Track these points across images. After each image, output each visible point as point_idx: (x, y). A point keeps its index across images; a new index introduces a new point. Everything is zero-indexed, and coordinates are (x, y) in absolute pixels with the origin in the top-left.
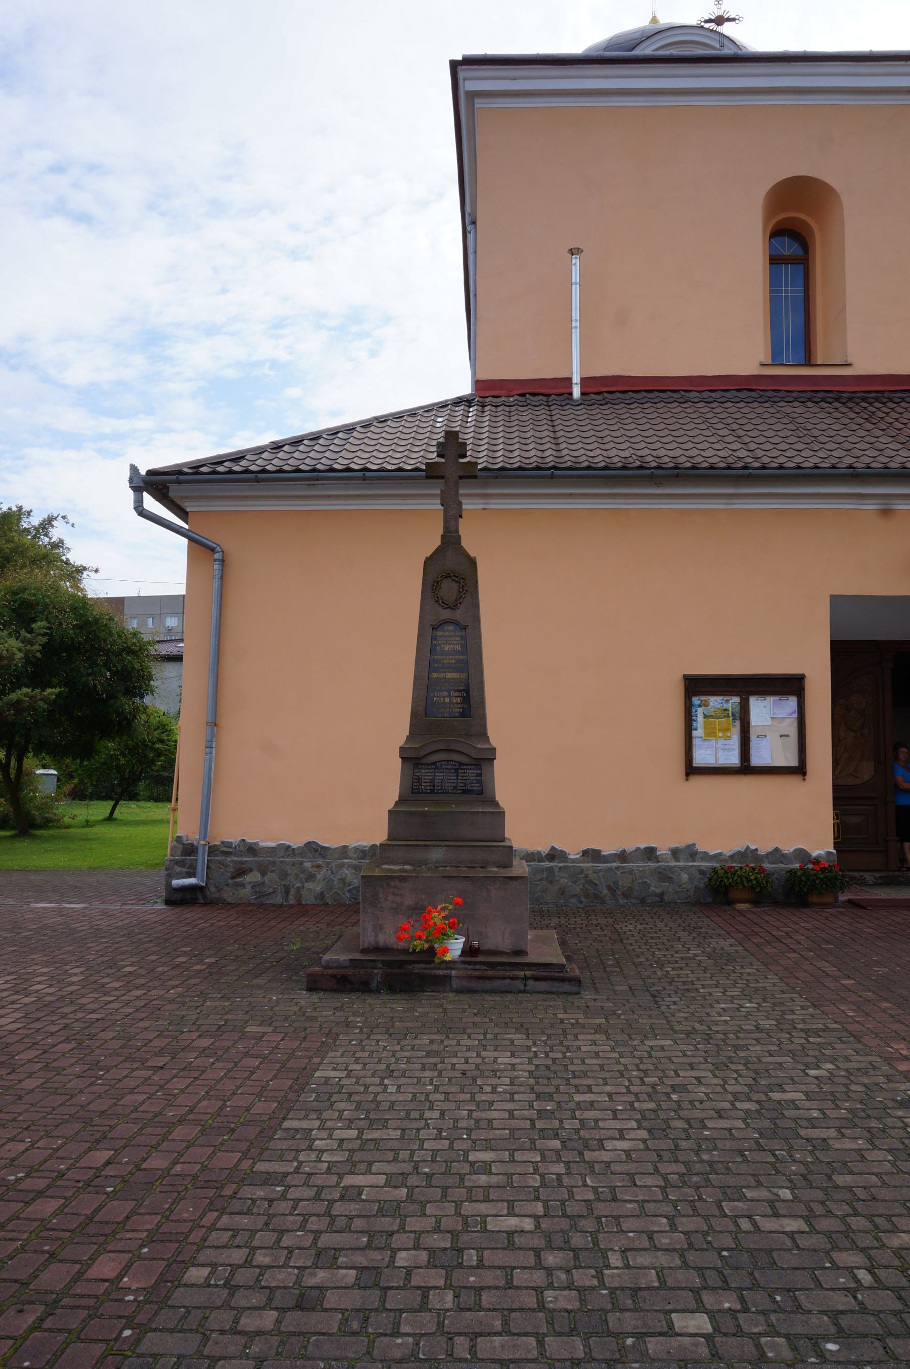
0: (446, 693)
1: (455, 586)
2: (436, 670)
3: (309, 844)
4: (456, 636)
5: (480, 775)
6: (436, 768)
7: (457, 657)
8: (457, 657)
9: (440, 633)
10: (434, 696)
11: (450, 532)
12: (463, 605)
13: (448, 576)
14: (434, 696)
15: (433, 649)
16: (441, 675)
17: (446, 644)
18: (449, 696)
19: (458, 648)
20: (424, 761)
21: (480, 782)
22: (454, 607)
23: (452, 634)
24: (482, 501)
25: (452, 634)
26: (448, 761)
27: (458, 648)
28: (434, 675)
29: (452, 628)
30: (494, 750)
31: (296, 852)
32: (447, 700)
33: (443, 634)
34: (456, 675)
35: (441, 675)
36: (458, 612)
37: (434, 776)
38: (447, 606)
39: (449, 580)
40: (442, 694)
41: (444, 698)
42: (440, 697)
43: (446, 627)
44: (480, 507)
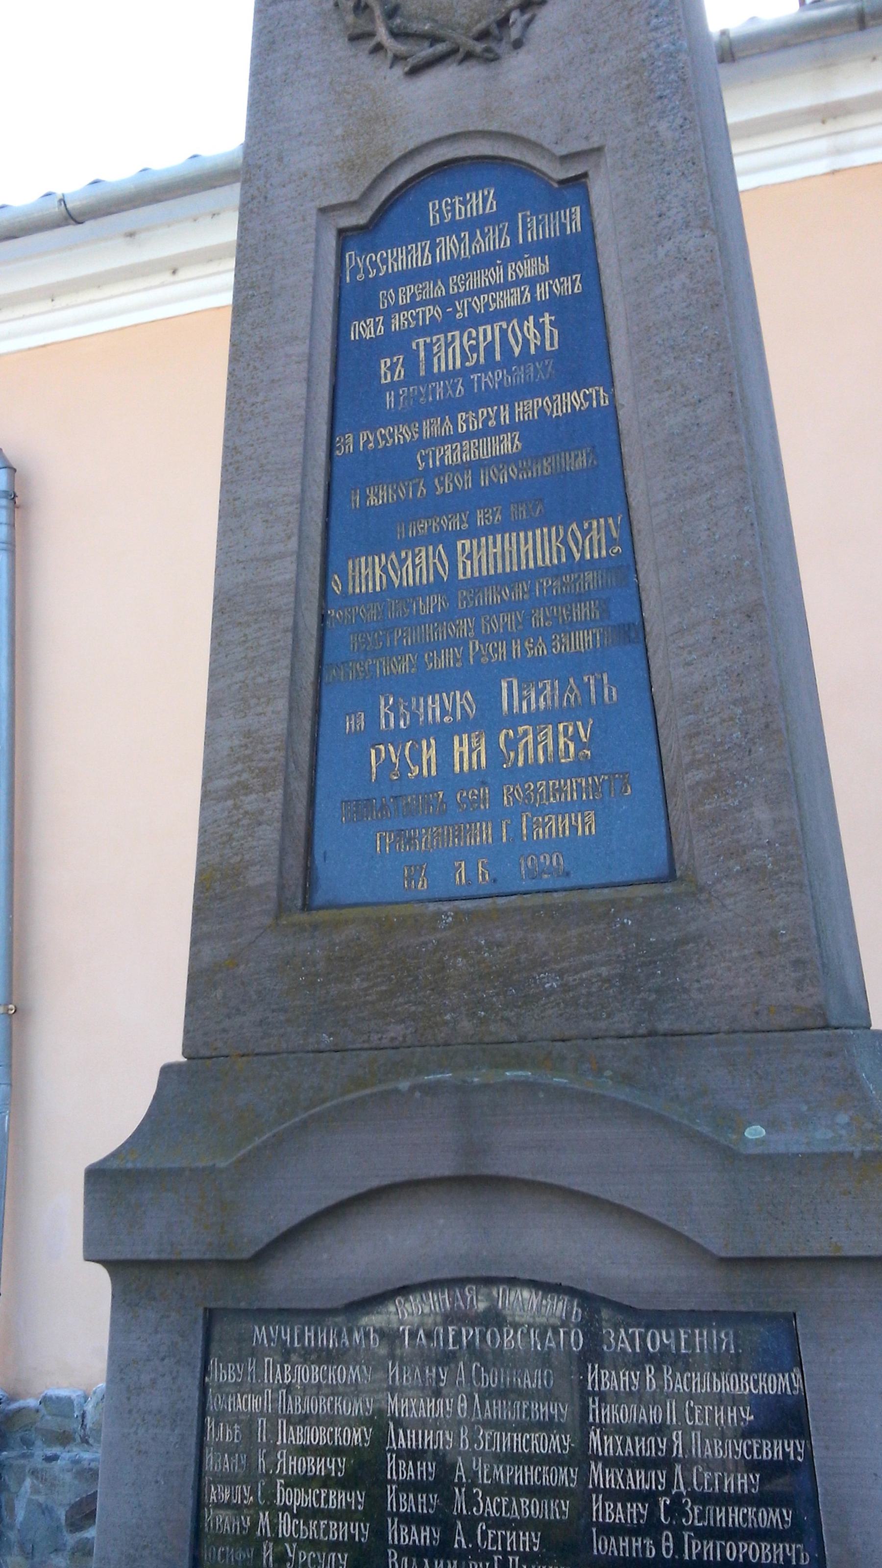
0: (463, 701)
2: (383, 535)
4: (515, 253)
5: (787, 1417)
7: (527, 409)
8: (527, 409)
10: (376, 736)
15: (348, 383)
16: (418, 567)
17: (448, 324)
18: (488, 720)
20: (285, 1281)
23: (493, 240)
24: (822, 145)
25: (493, 240)
27: (539, 334)
28: (368, 573)
32: (468, 753)
33: (418, 256)
34: (535, 548)
35: (418, 567)
36: (519, 68)
40: (432, 708)
41: (444, 735)
42: (417, 732)
44: (821, 167)
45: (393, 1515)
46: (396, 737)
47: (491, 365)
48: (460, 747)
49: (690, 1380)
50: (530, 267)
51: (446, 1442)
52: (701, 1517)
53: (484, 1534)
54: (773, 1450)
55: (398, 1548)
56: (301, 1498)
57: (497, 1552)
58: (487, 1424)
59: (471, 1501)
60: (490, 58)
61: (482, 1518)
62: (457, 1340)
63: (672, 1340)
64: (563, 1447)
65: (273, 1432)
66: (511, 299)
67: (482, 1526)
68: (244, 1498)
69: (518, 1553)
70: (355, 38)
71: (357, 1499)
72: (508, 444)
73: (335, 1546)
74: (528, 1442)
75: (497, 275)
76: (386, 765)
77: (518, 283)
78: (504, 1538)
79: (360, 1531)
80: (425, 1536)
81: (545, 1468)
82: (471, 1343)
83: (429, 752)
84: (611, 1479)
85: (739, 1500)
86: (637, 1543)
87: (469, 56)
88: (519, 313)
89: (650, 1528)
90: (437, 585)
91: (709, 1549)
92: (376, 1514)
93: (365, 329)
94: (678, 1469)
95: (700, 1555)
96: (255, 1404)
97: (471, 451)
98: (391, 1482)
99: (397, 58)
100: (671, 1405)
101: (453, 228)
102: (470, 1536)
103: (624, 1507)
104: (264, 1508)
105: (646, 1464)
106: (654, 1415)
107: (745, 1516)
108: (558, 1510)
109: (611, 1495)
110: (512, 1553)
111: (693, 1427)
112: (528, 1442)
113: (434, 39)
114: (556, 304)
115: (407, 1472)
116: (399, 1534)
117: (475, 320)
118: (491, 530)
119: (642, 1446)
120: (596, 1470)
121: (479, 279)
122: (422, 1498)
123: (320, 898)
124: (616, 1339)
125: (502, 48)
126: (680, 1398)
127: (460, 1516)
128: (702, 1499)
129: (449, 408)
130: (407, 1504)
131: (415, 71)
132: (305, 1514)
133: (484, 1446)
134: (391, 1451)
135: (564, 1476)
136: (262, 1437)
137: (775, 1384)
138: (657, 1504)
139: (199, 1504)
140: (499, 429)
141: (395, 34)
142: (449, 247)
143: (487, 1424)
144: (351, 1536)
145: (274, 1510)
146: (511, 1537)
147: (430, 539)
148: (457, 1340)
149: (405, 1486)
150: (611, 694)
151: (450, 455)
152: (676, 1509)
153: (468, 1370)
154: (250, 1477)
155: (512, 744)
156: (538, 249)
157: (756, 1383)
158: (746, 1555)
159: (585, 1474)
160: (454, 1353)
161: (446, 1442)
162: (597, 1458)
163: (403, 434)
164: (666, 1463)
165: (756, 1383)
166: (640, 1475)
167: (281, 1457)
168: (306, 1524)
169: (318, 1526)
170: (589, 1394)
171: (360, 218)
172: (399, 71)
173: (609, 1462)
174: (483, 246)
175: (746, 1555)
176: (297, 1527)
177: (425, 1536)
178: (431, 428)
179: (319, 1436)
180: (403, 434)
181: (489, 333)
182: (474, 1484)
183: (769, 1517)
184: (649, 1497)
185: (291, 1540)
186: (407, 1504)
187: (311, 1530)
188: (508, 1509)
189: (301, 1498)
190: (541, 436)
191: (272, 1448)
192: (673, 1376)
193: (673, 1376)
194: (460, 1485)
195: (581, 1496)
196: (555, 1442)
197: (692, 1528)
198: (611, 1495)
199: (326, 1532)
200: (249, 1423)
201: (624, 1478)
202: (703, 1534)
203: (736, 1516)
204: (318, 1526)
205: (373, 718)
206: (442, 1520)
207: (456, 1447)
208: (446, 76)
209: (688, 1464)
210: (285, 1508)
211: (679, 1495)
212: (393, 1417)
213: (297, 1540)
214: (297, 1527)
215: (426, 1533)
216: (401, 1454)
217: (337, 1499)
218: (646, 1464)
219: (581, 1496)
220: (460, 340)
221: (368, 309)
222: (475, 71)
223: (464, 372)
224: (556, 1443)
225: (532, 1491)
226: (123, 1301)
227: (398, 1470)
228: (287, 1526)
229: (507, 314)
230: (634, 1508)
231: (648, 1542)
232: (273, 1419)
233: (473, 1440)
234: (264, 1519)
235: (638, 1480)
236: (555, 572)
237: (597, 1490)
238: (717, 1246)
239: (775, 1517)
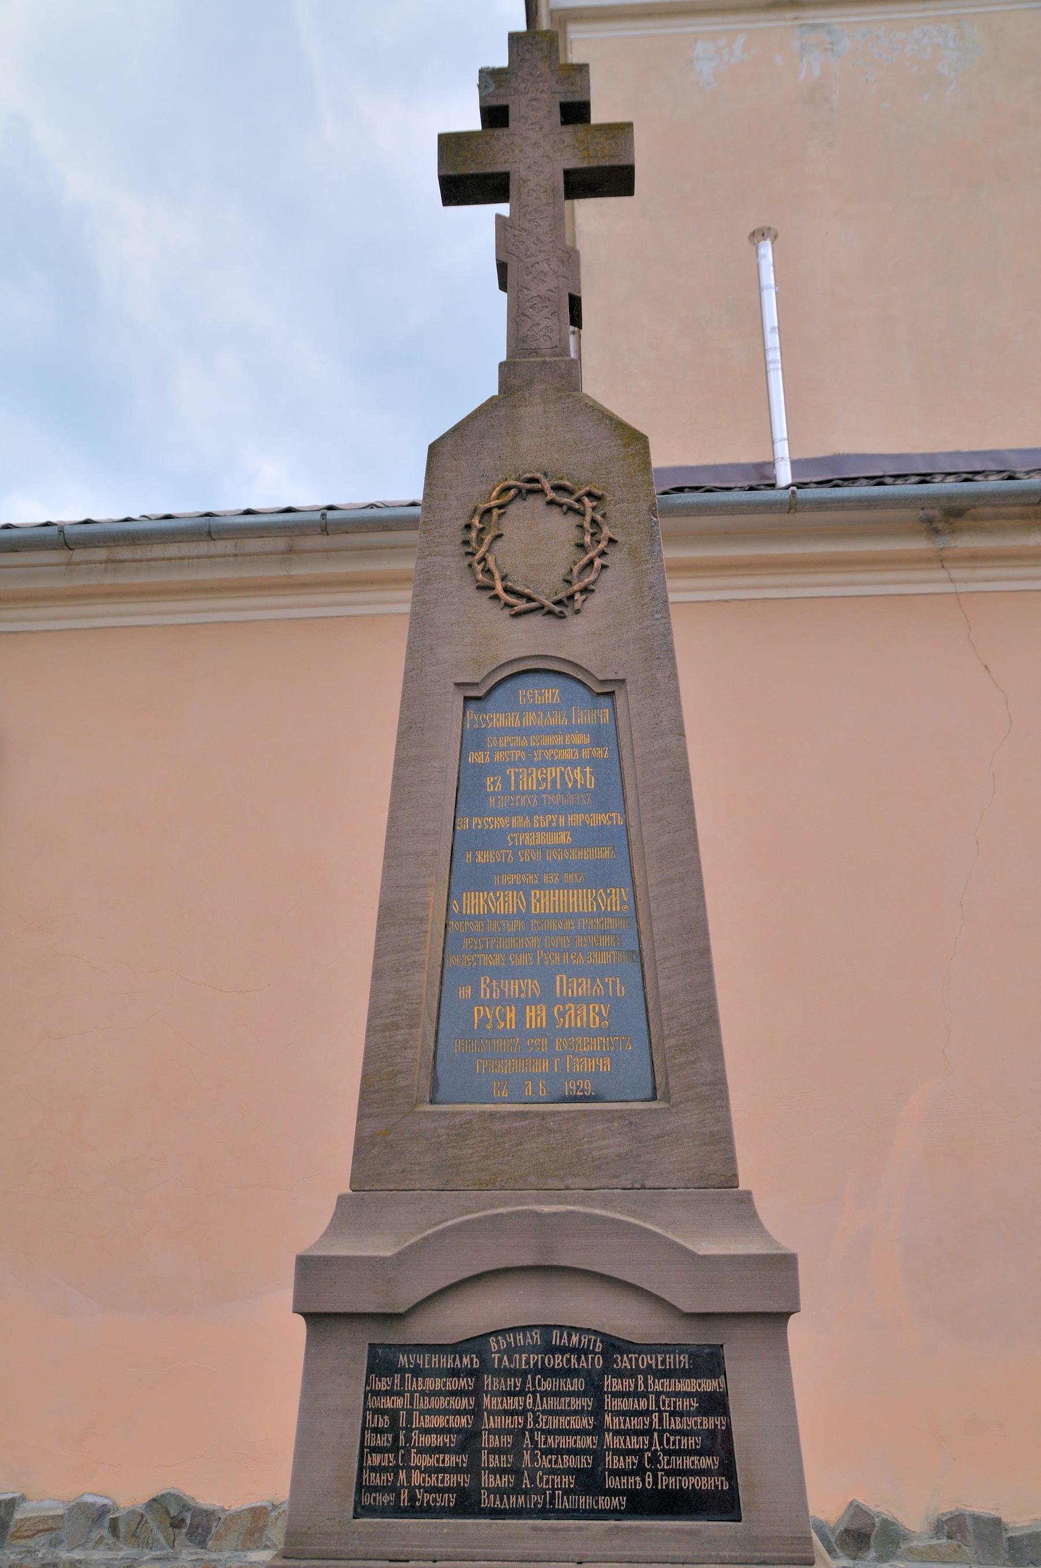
0: (533, 986)
1: (561, 528)
2: (482, 880)
3: (158, 1503)
4: (570, 729)
5: (716, 1404)
6: (485, 1367)
7: (576, 819)
8: (576, 819)
9: (498, 719)
10: (476, 999)
11: (535, 352)
12: (595, 601)
13: (530, 488)
14: (476, 999)
15: (467, 791)
16: (506, 903)
17: (529, 763)
18: (548, 997)
19: (583, 778)
21: (720, 1444)
22: (560, 608)
23: (556, 720)
25: (556, 720)
26: (547, 1329)
27: (583, 778)
28: (474, 902)
29: (550, 693)
30: (785, 1264)
31: (122, 1528)
32: (535, 1017)
34: (579, 900)
35: (506, 903)
36: (576, 626)
37: (476, 1412)
38: (522, 604)
39: (536, 503)
40: (513, 987)
41: (521, 1005)
42: (503, 1001)
43: (530, 692)
45: (485, 1469)
46: (490, 1003)
47: (554, 791)
48: (530, 1012)
49: (663, 1384)
50: (579, 739)
51: (519, 1424)
52: (668, 1463)
53: (541, 1478)
54: (709, 1423)
55: (488, 1489)
56: (428, 1461)
57: (548, 1489)
58: (544, 1412)
59: (534, 1458)
60: (561, 616)
61: (540, 1469)
62: (528, 1363)
63: (654, 1361)
64: (589, 1425)
65: (409, 1421)
66: (567, 755)
67: (540, 1473)
68: (389, 1462)
69: (561, 1489)
70: (482, 588)
71: (464, 1460)
72: (564, 838)
73: (449, 1490)
74: (569, 1422)
75: (560, 741)
76: (484, 1020)
77: (572, 746)
78: (553, 1480)
79: (464, 1480)
80: (505, 1481)
81: (579, 1437)
82: (536, 1364)
83: (511, 1015)
84: (618, 1442)
85: (689, 1453)
86: (631, 1480)
87: (550, 612)
88: (573, 764)
89: (639, 1471)
90: (519, 916)
91: (672, 1482)
92: (474, 1469)
93: (476, 757)
94: (656, 1434)
95: (667, 1486)
96: (399, 1402)
97: (541, 839)
98: (485, 1448)
99: (507, 605)
100: (652, 1397)
101: (534, 708)
102: (532, 1480)
103: (624, 1459)
104: (402, 1468)
105: (637, 1433)
106: (643, 1404)
107: (693, 1462)
108: (584, 1462)
109: (617, 1452)
110: (557, 1489)
111: (665, 1411)
112: (569, 1422)
113: (530, 599)
114: (593, 762)
115: (495, 1442)
116: (489, 1481)
117: (545, 764)
118: (552, 887)
119: (635, 1423)
120: (608, 1437)
121: (549, 740)
122: (503, 1458)
123: (439, 1097)
124: (622, 1361)
125: (567, 612)
126: (658, 1394)
127: (527, 1468)
128: (669, 1453)
129: (528, 812)
130: (494, 1461)
131: (517, 615)
132: (429, 1471)
133: (542, 1425)
134: (485, 1430)
135: (589, 1442)
136: (402, 1423)
137: (709, 1385)
138: (643, 1456)
139: (361, 1468)
140: (558, 829)
141: (506, 590)
142: (530, 719)
143: (544, 1412)
144: (459, 1483)
145: (409, 1469)
146: (557, 1479)
147: (514, 887)
148: (528, 1363)
149: (492, 1451)
150: (621, 991)
151: (528, 839)
152: (654, 1459)
153: (533, 1379)
154: (394, 1448)
155: (562, 1015)
156: (584, 729)
157: (700, 1385)
158: (693, 1485)
159: (601, 1441)
160: (525, 1370)
161: (519, 1424)
162: (609, 1430)
163: (501, 822)
164: (648, 1432)
165: (700, 1385)
166: (634, 1439)
167: (415, 1435)
168: (430, 1476)
169: (437, 1478)
170: (605, 1393)
171: (480, 693)
172: (507, 612)
173: (617, 1433)
174: (553, 721)
175: (693, 1485)
176: (424, 1479)
177: (505, 1481)
178: (517, 822)
179: (440, 1421)
180: (501, 822)
181: (553, 772)
182: (536, 1448)
183: (706, 1462)
184: (638, 1453)
185: (420, 1487)
186: (494, 1461)
187: (432, 1481)
188: (556, 1463)
189: (428, 1461)
190: (585, 837)
191: (409, 1430)
192: (654, 1382)
193: (654, 1382)
194: (527, 1449)
195: (598, 1454)
196: (585, 1421)
197: (663, 1470)
198: (617, 1452)
199: (442, 1481)
200: (393, 1414)
201: (625, 1442)
202: (669, 1473)
203: (688, 1462)
204: (437, 1478)
205: (476, 991)
206: (516, 1471)
207: (525, 1426)
208: (536, 621)
209: (661, 1432)
210: (417, 1467)
211: (656, 1450)
212: (486, 1409)
213: (424, 1487)
214: (424, 1479)
215: (505, 1478)
216: (491, 1431)
217: (450, 1460)
218: (637, 1433)
219: (598, 1454)
220: (536, 774)
221: (479, 747)
222: (551, 621)
223: (538, 793)
224: (586, 1422)
225: (570, 1452)
226: (312, 1341)
227: (489, 1441)
228: (417, 1478)
229: (565, 763)
230: (629, 1460)
231: (638, 1479)
232: (410, 1413)
233: (536, 1421)
234: (402, 1475)
235: (633, 1443)
236: (591, 916)
237: (608, 1449)
238: (687, 1305)
239: (709, 1462)
